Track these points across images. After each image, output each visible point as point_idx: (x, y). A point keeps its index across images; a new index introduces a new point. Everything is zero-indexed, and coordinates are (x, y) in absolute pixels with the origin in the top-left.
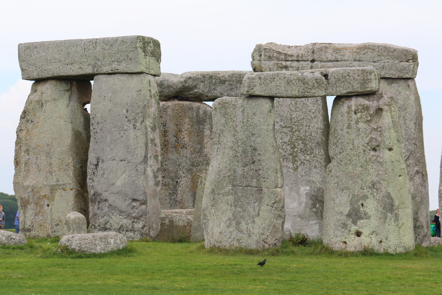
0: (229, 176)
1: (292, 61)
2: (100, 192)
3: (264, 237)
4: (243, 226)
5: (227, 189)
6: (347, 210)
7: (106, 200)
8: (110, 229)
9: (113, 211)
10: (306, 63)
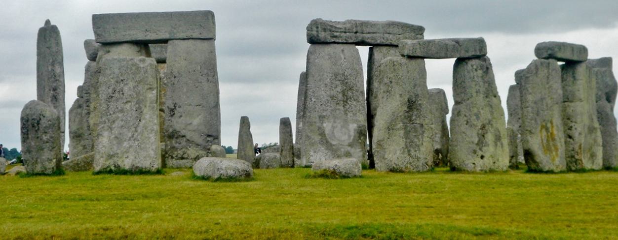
0: (401, 116)
2: (178, 129)
3: (427, 160)
4: (413, 153)
5: (398, 126)
6: (476, 140)
7: (184, 136)
8: (187, 158)
9: (190, 145)
10: (352, 34)
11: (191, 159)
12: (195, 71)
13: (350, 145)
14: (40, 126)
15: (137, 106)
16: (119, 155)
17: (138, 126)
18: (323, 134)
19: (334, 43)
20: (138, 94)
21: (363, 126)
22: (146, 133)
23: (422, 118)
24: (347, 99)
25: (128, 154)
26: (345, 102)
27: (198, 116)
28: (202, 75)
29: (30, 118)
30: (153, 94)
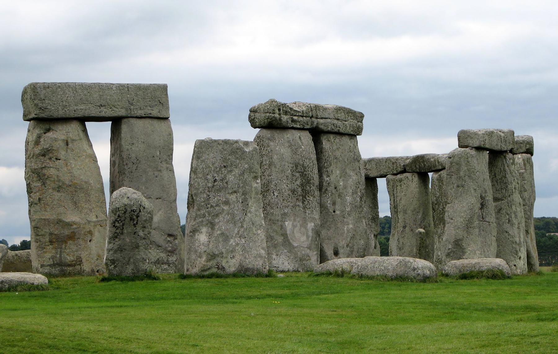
13: (309, 248)
15: (243, 197)
16: (224, 255)
17: (244, 220)
18: (285, 235)
20: (245, 183)
22: (254, 229)
24: (306, 194)
25: (234, 254)
27: (158, 212)
29: (129, 210)
30: (257, 183)
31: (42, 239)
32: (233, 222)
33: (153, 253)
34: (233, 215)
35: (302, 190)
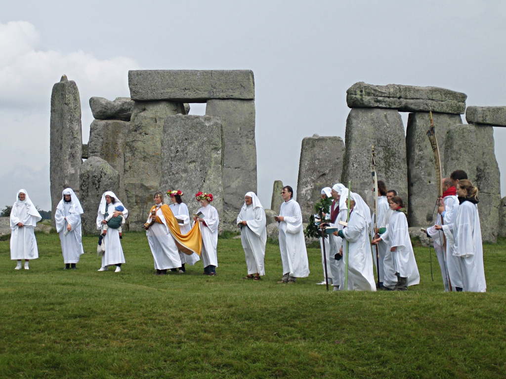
1: (384, 97)
3: (494, 230)
10: (395, 99)
11: (229, 222)
12: (234, 132)
14: (100, 183)
17: (202, 186)
19: (378, 107)
20: (203, 154)
21: (404, 193)
23: (490, 187)
24: (389, 166)
26: (387, 169)
27: (237, 179)
28: (241, 137)
29: (91, 175)
30: (218, 154)
31: (131, 200)
32: (190, 188)
33: (230, 214)
34: (191, 182)
35: (385, 162)
